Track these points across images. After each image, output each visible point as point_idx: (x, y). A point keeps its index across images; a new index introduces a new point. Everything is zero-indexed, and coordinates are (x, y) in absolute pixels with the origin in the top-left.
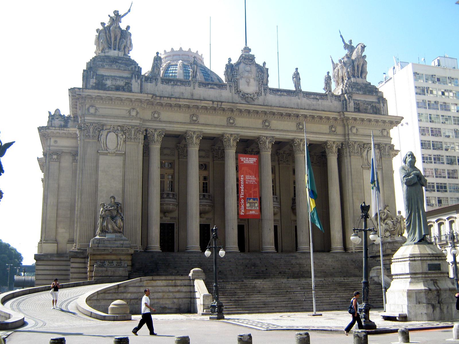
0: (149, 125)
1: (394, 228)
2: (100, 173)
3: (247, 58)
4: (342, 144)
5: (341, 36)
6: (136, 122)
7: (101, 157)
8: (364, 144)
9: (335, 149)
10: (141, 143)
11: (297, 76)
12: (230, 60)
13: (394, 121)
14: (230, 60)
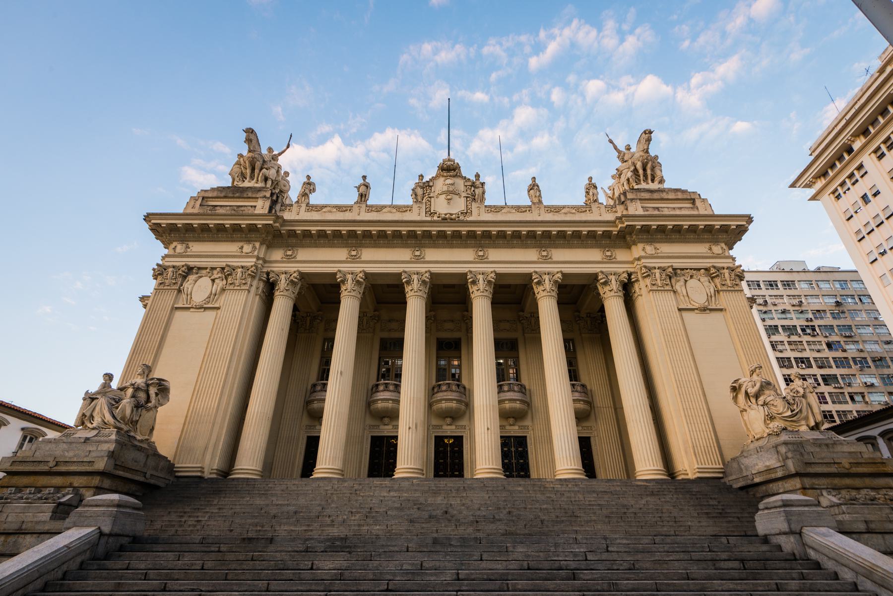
0: (277, 268)
4: (630, 275)
5: (611, 141)
6: (250, 262)
7: (178, 314)
8: (674, 269)
9: (614, 285)
11: (534, 187)
14: (421, 177)
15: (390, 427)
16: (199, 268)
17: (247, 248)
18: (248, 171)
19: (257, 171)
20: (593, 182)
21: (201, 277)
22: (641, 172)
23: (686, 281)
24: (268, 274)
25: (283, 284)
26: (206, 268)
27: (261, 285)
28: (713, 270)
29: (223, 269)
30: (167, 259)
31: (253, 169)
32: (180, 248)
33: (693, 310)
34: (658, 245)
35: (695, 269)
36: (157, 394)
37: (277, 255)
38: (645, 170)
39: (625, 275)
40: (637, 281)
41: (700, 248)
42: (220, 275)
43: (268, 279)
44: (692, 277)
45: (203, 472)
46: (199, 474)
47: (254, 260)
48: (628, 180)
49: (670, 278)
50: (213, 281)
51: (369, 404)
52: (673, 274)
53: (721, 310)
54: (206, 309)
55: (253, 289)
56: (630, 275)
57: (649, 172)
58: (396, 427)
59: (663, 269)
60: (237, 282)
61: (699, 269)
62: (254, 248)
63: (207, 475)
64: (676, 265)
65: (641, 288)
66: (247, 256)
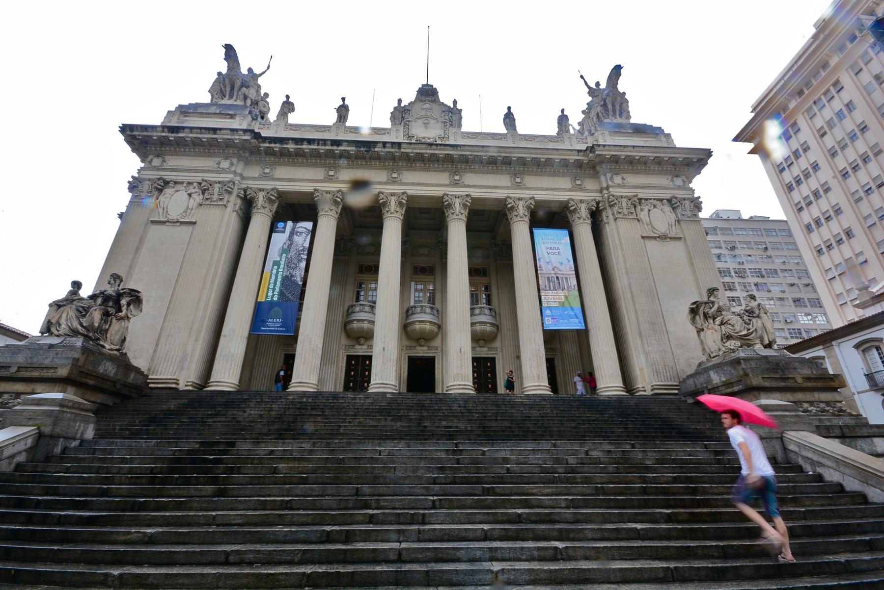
0: (254, 184)
1: (748, 330)
2: (144, 251)
3: (428, 93)
4: (598, 203)
5: (582, 77)
8: (640, 199)
9: (584, 212)
12: (400, 101)
13: (695, 157)
14: (400, 101)
15: (365, 347)
16: (176, 183)
17: (225, 164)
18: (228, 89)
19: (236, 89)
20: (565, 113)
21: (177, 191)
22: (610, 107)
24: (245, 191)
25: (261, 199)
26: (183, 183)
27: (239, 202)
28: (674, 201)
29: (200, 184)
30: (142, 172)
31: (232, 88)
32: (157, 162)
33: (655, 238)
34: (624, 176)
35: (658, 200)
36: (129, 304)
37: (254, 171)
38: (613, 105)
39: (594, 204)
40: (605, 209)
41: (662, 180)
42: (196, 190)
43: (246, 196)
44: (655, 207)
45: (178, 384)
46: (174, 386)
47: (231, 176)
48: (598, 114)
50: (190, 195)
51: (346, 324)
52: (637, 202)
53: (680, 238)
54: (182, 223)
55: (230, 206)
56: (598, 203)
57: (618, 107)
58: (371, 347)
60: (215, 197)
61: (661, 200)
62: (232, 164)
63: (182, 387)
64: (640, 196)
65: (608, 216)
66: (224, 171)
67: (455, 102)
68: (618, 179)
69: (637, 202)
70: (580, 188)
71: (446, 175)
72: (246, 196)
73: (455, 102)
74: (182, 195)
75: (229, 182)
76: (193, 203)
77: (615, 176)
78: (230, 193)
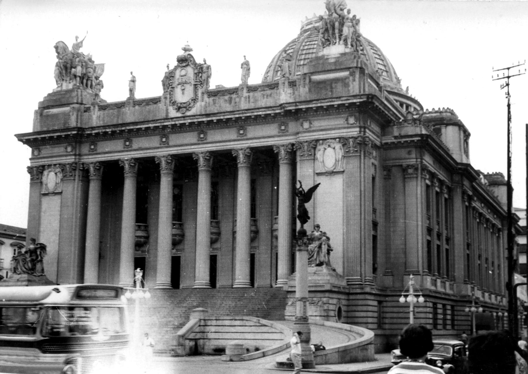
10: (76, 181)
21: (50, 171)
23: (325, 149)
39: (290, 146)
43: (84, 168)
44: (329, 146)
47: (73, 157)
49: (315, 148)
50: (56, 174)
52: (314, 144)
55: (77, 177)
56: (293, 145)
59: (309, 142)
61: (335, 139)
67: (205, 61)
68: (306, 125)
69: (314, 144)
70: (283, 133)
71: (196, 133)
72: (84, 168)
73: (205, 61)
74: (52, 174)
75: (73, 163)
76: (59, 180)
77: (304, 122)
78: (75, 170)
